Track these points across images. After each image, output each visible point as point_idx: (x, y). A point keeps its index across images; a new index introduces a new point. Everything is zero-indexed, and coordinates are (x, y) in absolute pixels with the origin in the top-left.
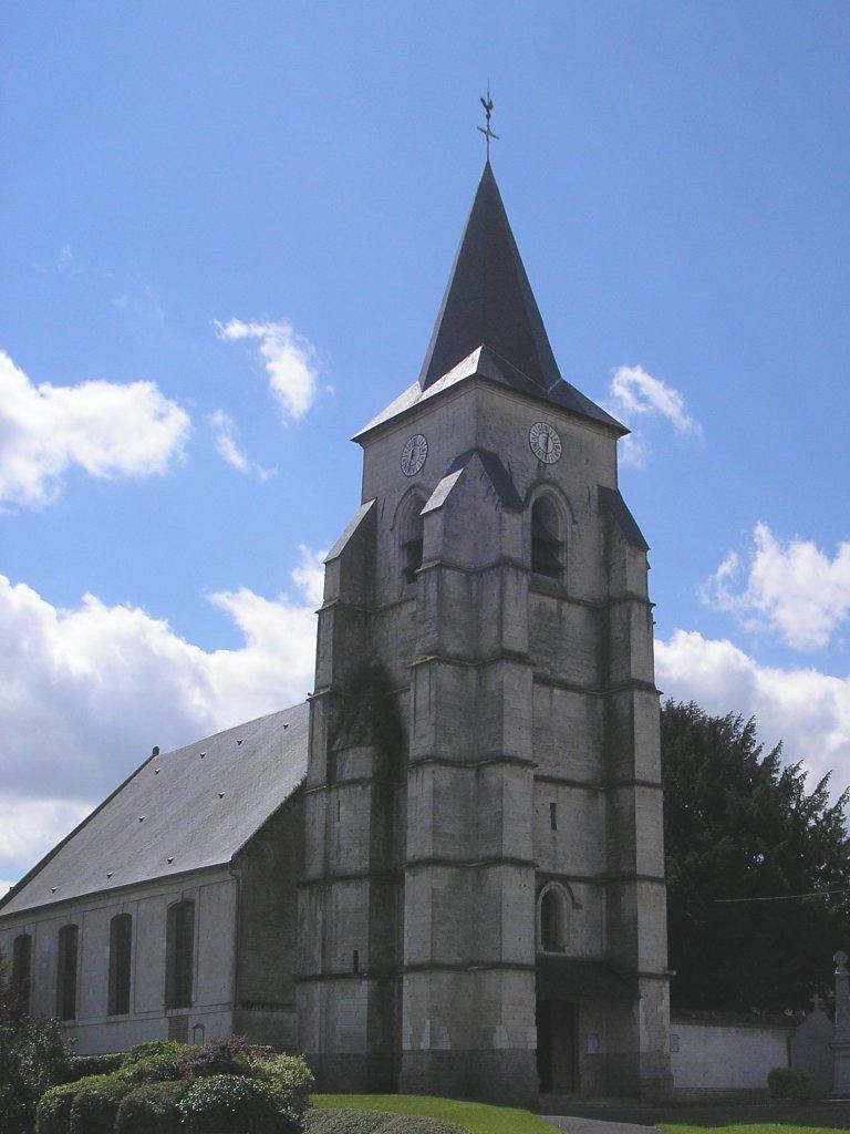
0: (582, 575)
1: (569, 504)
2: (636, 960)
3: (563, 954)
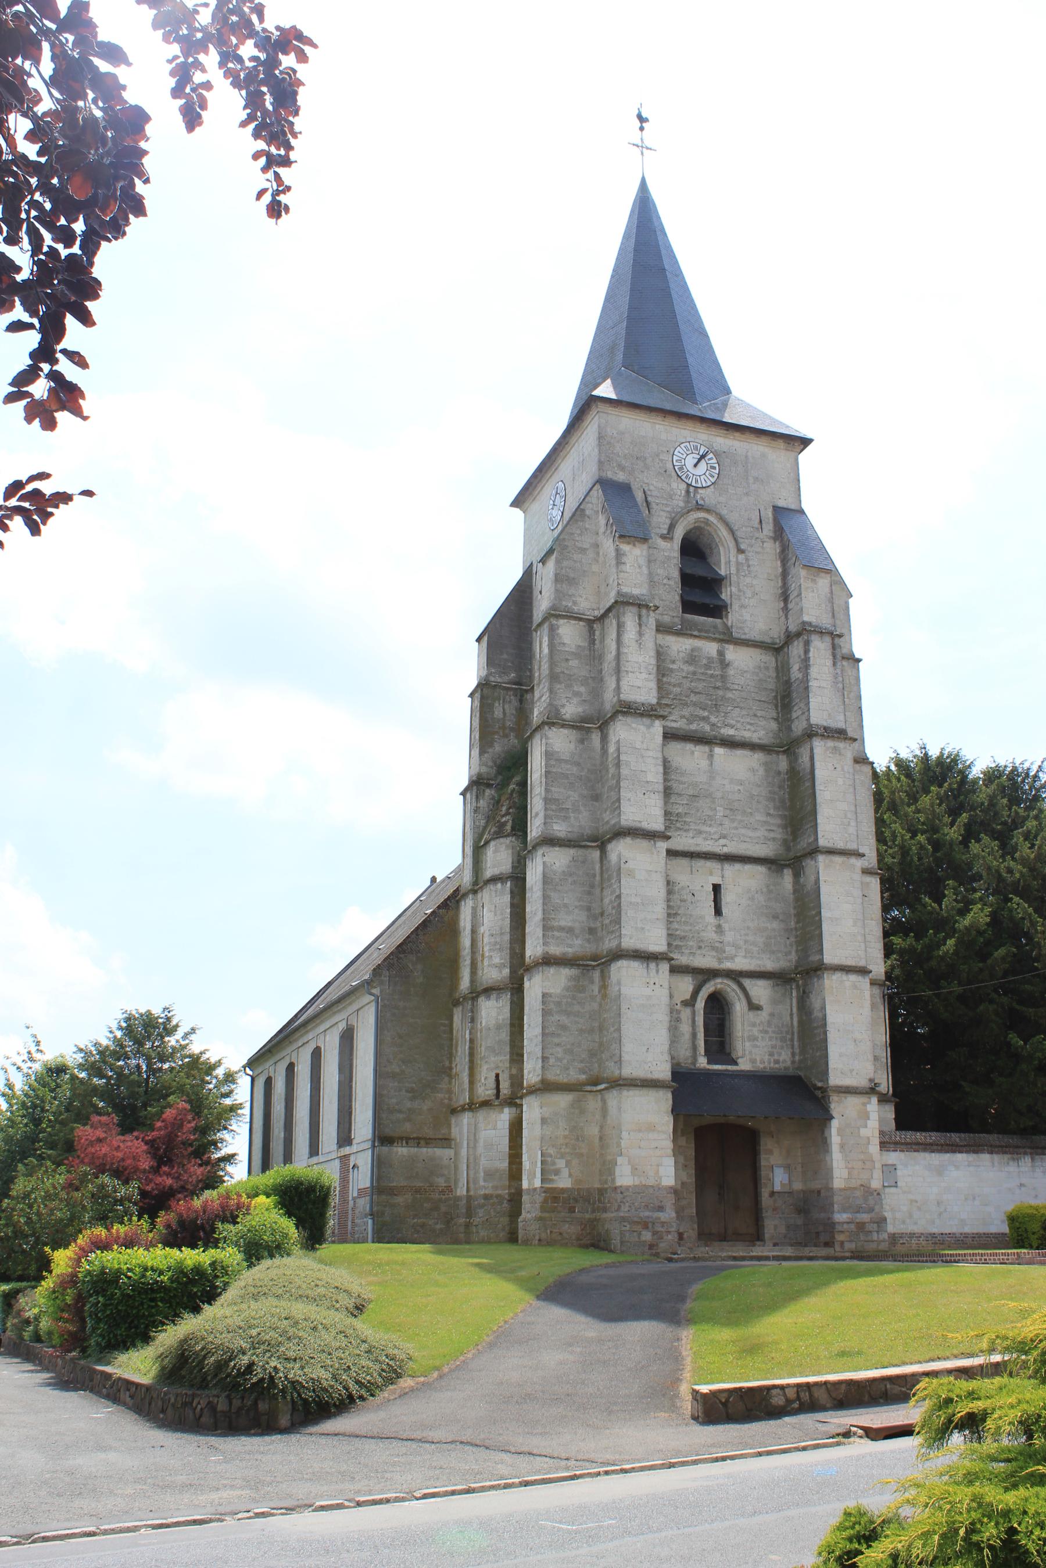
0: (751, 606)
1: (732, 532)
2: (825, 1072)
3: (735, 1068)
